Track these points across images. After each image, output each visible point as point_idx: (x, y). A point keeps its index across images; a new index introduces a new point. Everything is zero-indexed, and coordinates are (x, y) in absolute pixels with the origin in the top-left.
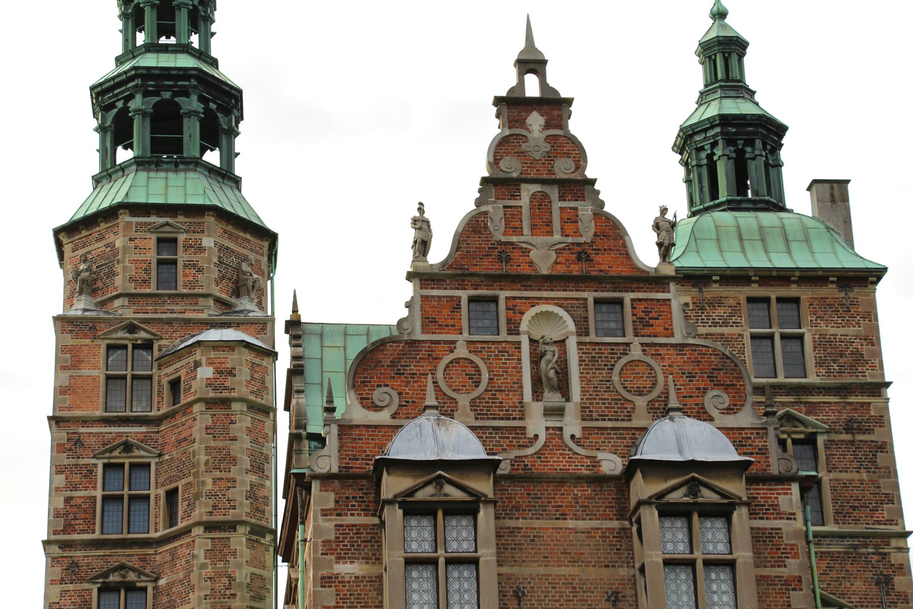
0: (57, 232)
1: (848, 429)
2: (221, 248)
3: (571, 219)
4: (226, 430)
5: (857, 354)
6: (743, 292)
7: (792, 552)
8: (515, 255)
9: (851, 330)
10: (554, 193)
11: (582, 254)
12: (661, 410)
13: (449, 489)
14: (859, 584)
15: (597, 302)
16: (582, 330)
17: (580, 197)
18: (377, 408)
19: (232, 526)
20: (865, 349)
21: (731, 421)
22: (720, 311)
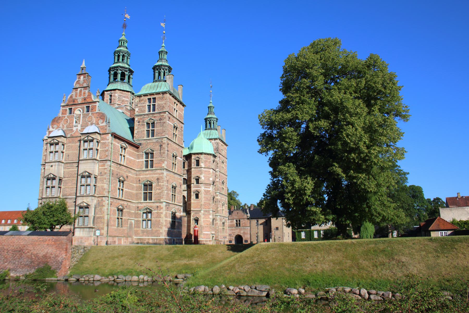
1: (160, 120)
3: (84, 93)
6: (147, 98)
8: (76, 101)
11: (85, 99)
12: (92, 124)
13: (55, 141)
14: (158, 147)
16: (83, 112)
17: (86, 89)
20: (165, 105)
21: (102, 125)
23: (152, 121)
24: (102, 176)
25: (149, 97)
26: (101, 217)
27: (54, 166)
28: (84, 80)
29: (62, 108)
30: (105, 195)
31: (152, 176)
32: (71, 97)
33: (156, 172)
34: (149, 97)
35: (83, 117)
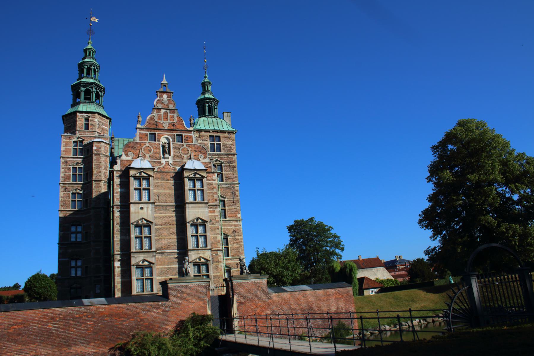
0: (63, 117)
2: (99, 121)
3: (172, 117)
4: (99, 160)
5: (231, 148)
6: (209, 134)
7: (215, 187)
8: (160, 125)
9: (230, 143)
10: (168, 111)
13: (143, 174)
15: (177, 135)
16: (174, 141)
18: (128, 156)
19: (100, 181)
20: (232, 147)
22: (204, 138)
23: (219, 163)
24: (213, 224)
25: (211, 134)
26: (217, 276)
27: (145, 209)
28: (168, 100)
29: (138, 131)
30: (221, 249)
31: (225, 228)
32: (152, 118)
33: (231, 223)
34: (211, 134)
35: (175, 148)
